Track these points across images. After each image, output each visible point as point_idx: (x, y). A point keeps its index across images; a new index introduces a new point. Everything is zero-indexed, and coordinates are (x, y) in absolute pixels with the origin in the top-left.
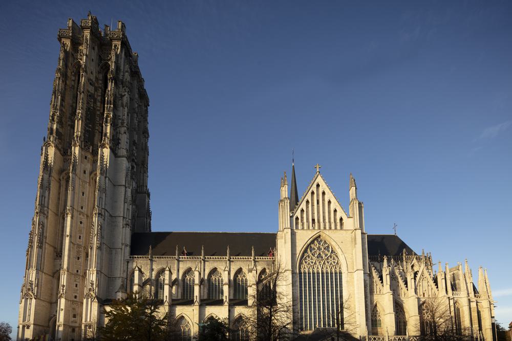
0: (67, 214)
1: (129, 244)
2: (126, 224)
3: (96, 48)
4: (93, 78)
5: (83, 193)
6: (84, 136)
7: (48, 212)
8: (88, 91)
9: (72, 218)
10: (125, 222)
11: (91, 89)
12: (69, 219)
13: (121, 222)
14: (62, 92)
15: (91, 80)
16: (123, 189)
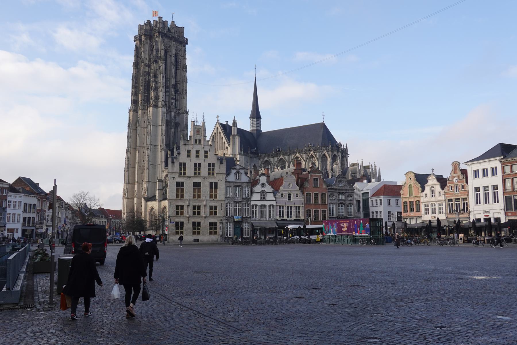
0: (137, 151)
1: (163, 160)
2: (162, 149)
3: (148, 41)
4: (147, 62)
5: (144, 135)
6: (144, 100)
7: (131, 150)
8: (145, 72)
9: (138, 152)
10: (161, 148)
11: (147, 69)
12: (137, 153)
13: (159, 148)
14: (136, 75)
15: (146, 63)
16: (160, 127)
